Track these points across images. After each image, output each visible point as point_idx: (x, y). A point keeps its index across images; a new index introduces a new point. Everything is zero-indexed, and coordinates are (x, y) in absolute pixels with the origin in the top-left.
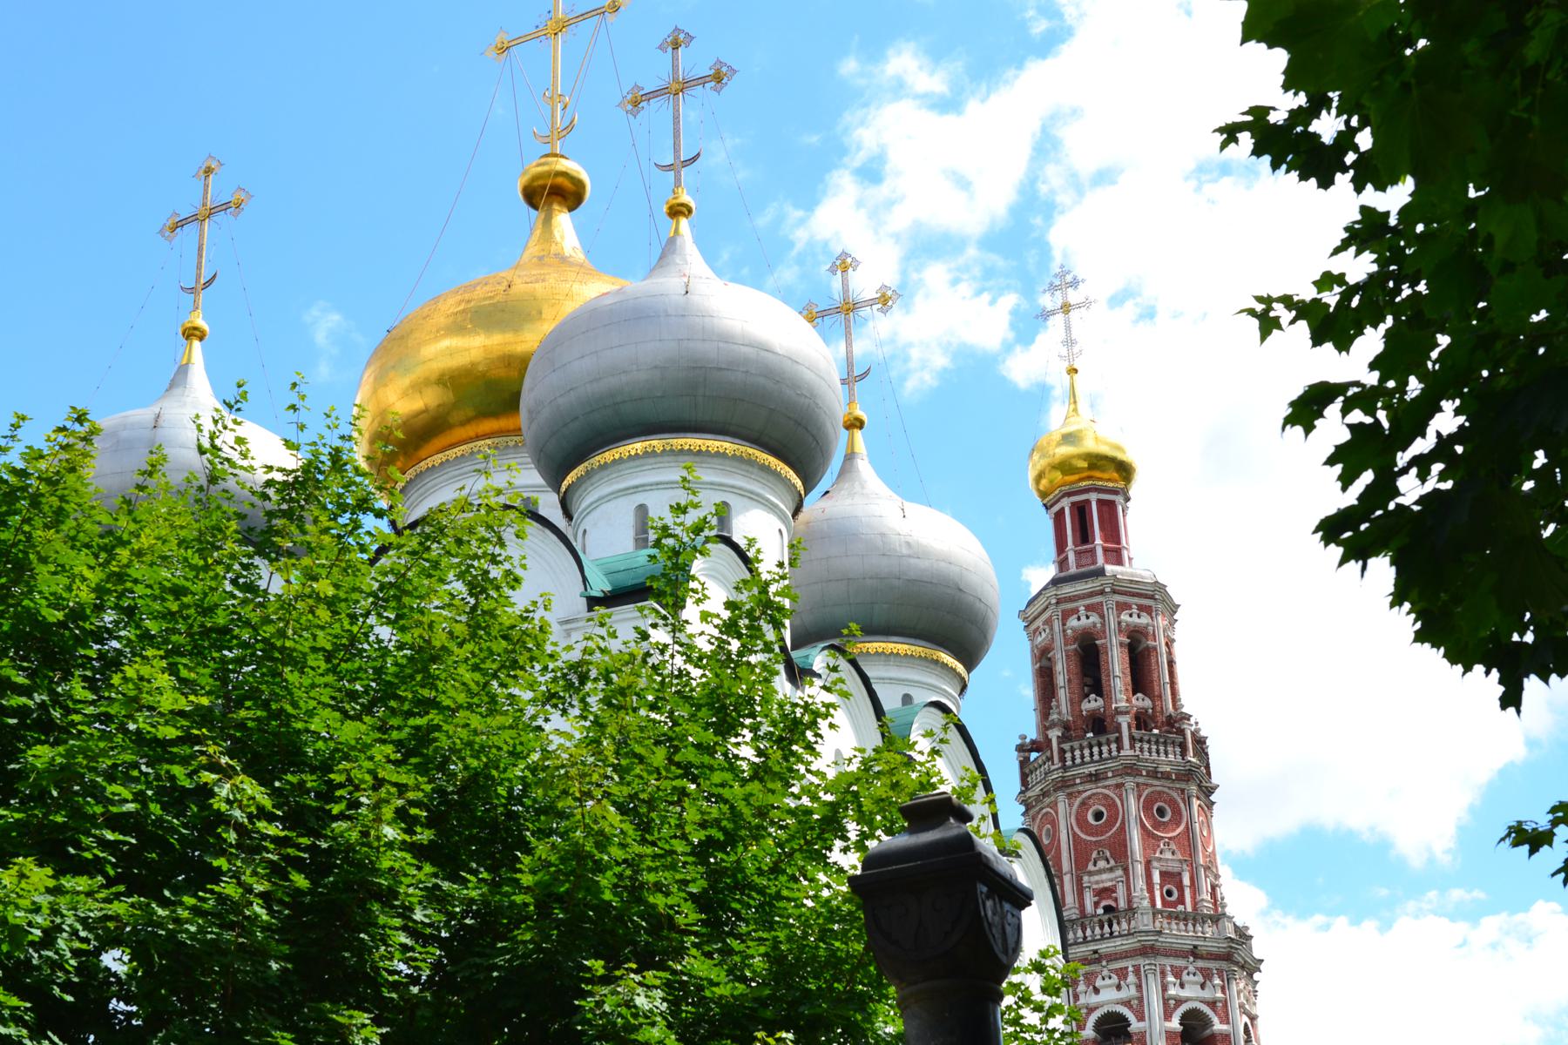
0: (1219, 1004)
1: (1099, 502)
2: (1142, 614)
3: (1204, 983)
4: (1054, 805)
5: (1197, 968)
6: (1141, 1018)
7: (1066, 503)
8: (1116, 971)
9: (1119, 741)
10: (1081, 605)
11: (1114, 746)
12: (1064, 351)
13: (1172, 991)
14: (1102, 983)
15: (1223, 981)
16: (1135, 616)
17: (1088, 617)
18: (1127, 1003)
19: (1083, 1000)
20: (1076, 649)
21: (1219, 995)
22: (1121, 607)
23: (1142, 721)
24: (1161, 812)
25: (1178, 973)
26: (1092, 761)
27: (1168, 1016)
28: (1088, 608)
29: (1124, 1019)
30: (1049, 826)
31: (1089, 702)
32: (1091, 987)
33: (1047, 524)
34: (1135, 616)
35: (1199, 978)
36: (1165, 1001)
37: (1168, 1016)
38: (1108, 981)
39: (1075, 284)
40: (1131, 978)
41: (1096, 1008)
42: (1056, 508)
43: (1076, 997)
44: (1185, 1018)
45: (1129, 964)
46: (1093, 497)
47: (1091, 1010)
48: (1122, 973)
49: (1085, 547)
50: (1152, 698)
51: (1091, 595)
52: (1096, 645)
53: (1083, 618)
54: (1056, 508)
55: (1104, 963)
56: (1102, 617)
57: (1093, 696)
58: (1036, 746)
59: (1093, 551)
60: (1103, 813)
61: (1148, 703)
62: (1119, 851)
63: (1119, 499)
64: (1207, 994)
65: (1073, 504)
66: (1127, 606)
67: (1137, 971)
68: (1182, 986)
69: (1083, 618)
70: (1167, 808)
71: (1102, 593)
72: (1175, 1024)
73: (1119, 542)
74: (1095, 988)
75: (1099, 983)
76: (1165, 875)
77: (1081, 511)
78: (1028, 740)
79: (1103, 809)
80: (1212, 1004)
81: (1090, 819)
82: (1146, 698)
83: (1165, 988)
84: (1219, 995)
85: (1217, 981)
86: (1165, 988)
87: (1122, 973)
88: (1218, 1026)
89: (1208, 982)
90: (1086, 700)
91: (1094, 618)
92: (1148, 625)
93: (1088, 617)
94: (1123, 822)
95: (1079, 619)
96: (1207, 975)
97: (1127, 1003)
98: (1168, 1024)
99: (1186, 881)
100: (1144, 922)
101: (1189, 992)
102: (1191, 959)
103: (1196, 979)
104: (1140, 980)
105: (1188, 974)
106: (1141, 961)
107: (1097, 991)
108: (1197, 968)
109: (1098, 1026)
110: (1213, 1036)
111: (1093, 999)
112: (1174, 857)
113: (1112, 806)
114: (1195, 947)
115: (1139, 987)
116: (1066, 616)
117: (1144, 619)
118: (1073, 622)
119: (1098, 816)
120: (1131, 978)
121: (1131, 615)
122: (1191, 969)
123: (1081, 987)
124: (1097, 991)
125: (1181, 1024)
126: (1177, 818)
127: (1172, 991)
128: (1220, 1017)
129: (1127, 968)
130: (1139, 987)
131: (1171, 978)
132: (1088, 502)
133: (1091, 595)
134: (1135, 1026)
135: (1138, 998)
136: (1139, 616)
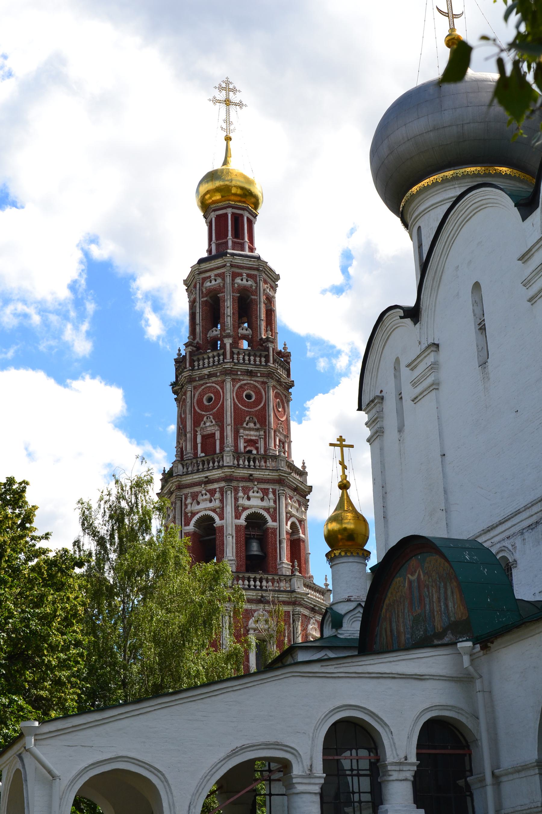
0: (272, 510)
1: (233, 214)
2: (249, 279)
3: (263, 497)
5: (258, 488)
6: (222, 518)
7: (213, 216)
8: (210, 491)
10: (212, 274)
11: (221, 357)
12: (224, 126)
14: (201, 498)
16: (245, 280)
17: (216, 281)
18: (214, 511)
22: (235, 275)
24: (249, 397)
25: (246, 490)
26: (209, 367)
27: (238, 516)
28: (216, 276)
29: (212, 520)
32: (195, 501)
33: (206, 228)
34: (245, 280)
35: (260, 494)
36: (237, 507)
37: (238, 517)
38: (205, 497)
39: (234, 90)
40: (217, 495)
41: (198, 513)
43: (186, 505)
44: (247, 518)
45: (216, 486)
46: (229, 211)
47: (194, 514)
48: (212, 492)
51: (218, 268)
52: (218, 297)
53: (213, 282)
54: (209, 220)
55: (203, 486)
56: (223, 279)
60: (212, 398)
62: (219, 418)
63: (246, 214)
64: (265, 504)
65: (218, 217)
66: (241, 275)
67: (222, 490)
68: (249, 499)
69: (213, 282)
70: (253, 394)
71: (224, 266)
72: (242, 521)
73: (243, 239)
75: (200, 498)
77: (221, 220)
79: (212, 395)
80: (267, 510)
81: (205, 403)
83: (236, 499)
84: (272, 503)
85: (271, 496)
86: (236, 499)
87: (212, 492)
88: (271, 523)
89: (265, 497)
90: (211, 331)
91: (219, 280)
92: (251, 286)
93: (216, 281)
94: (223, 404)
95: (211, 282)
96: (265, 492)
98: (237, 521)
100: (228, 460)
102: (256, 483)
103: (258, 495)
105: (253, 492)
106: (223, 484)
107: (198, 503)
108: (258, 488)
109: (198, 524)
110: (267, 529)
111: (196, 508)
113: (217, 393)
115: (222, 501)
116: (204, 279)
117: (250, 283)
118: (208, 284)
119: (210, 400)
120: (217, 495)
121: (242, 280)
122: (255, 489)
123: (189, 501)
127: (241, 502)
128: (272, 519)
129: (215, 489)
130: (222, 501)
131: (241, 494)
132: (226, 215)
133: (218, 268)
134: (218, 522)
135: (219, 508)
136: (247, 281)
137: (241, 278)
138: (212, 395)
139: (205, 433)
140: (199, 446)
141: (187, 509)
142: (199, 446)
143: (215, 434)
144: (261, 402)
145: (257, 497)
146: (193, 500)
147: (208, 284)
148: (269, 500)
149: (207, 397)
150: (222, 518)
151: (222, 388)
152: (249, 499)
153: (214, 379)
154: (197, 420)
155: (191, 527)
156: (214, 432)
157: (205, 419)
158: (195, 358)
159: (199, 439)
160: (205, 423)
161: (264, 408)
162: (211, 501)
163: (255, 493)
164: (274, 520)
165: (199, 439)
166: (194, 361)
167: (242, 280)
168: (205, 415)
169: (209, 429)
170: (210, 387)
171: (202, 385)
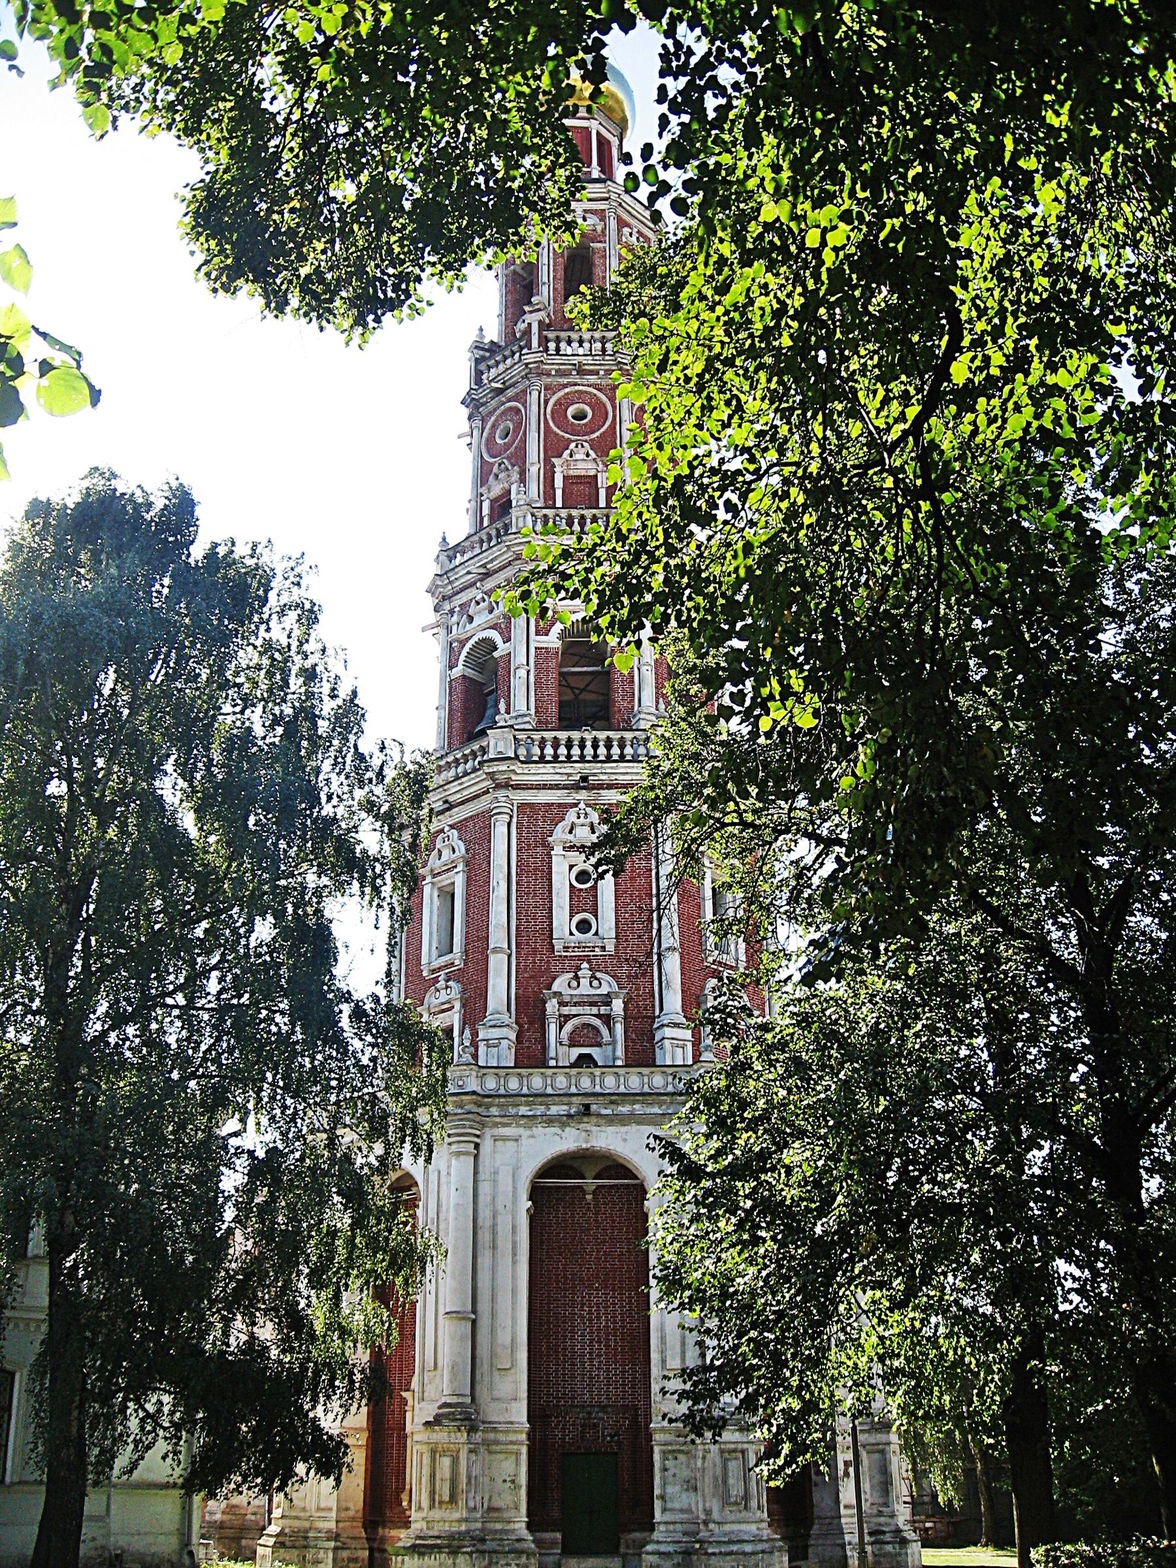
1: (598, 133)
4: (521, 397)
28: (585, 211)
58: (494, 348)
78: (486, 341)
113: (597, 406)
119: (580, 416)
138: (587, 409)
139: (571, 473)
140: (559, 493)
142: (559, 493)
151: (612, 399)
153: (593, 379)
154: (554, 448)
155: (553, 640)
156: (592, 473)
158: (551, 335)
159: (559, 482)
165: (559, 482)
166: (547, 340)
169: (581, 465)
170: (581, 392)
171: (565, 386)
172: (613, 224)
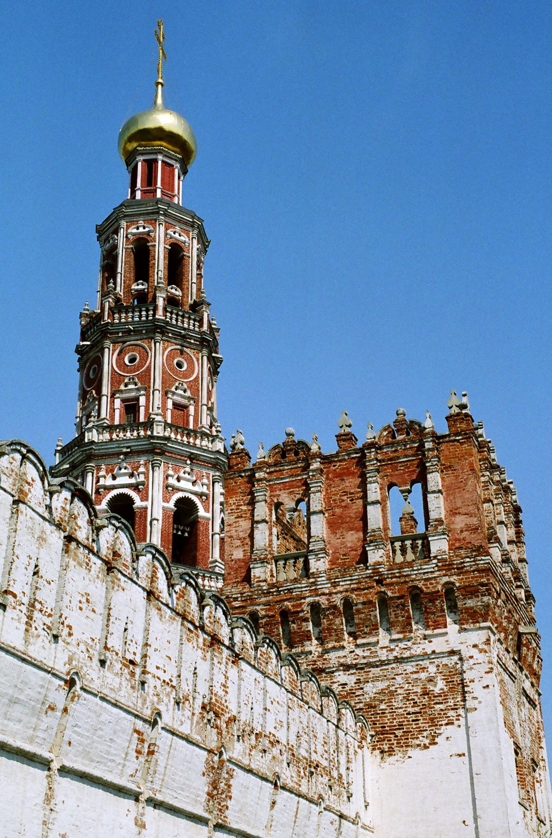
1: (163, 162)
6: (144, 498)
9: (155, 309)
11: (151, 312)
13: (172, 481)
15: (209, 481)
17: (144, 228)
18: (135, 487)
19: (102, 482)
20: (132, 248)
21: (205, 489)
23: (172, 301)
27: (166, 499)
29: (131, 501)
30: (96, 366)
31: (138, 285)
32: (110, 474)
38: (123, 471)
40: (142, 469)
42: (133, 165)
43: (98, 481)
46: (160, 157)
49: (149, 188)
50: (182, 290)
52: (148, 246)
54: (133, 165)
57: (141, 281)
59: (155, 191)
61: (179, 293)
64: (197, 489)
68: (178, 479)
71: (158, 213)
72: (171, 505)
73: (173, 191)
74: (113, 475)
76: (176, 406)
81: (127, 361)
82: (178, 289)
85: (205, 481)
88: (202, 512)
89: (198, 481)
90: (136, 284)
95: (138, 228)
97: (135, 487)
98: (166, 505)
99: (192, 409)
101: (183, 484)
104: (148, 471)
105: (184, 473)
107: (114, 478)
112: (186, 394)
114: (192, 453)
119: (132, 360)
121: (174, 233)
123: (103, 473)
124: (114, 478)
125: (175, 506)
126: (191, 370)
130: (147, 478)
132: (156, 161)
134: (138, 503)
137: (174, 230)
141: (98, 484)
143: (137, 399)
144: (193, 373)
145: (188, 480)
146: (107, 472)
147: (135, 231)
148: (203, 485)
149: (129, 356)
150: (144, 498)
152: (178, 479)
157: (126, 380)
160: (126, 385)
161: (197, 378)
162: (132, 475)
163: (186, 475)
164: (207, 510)
167: (174, 233)
168: (127, 376)
172: (162, 228)
